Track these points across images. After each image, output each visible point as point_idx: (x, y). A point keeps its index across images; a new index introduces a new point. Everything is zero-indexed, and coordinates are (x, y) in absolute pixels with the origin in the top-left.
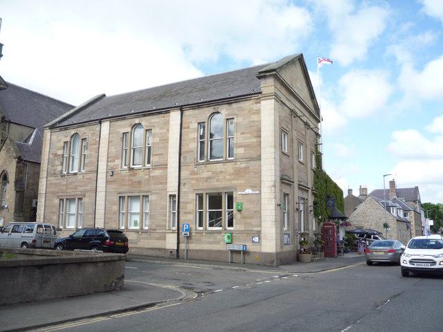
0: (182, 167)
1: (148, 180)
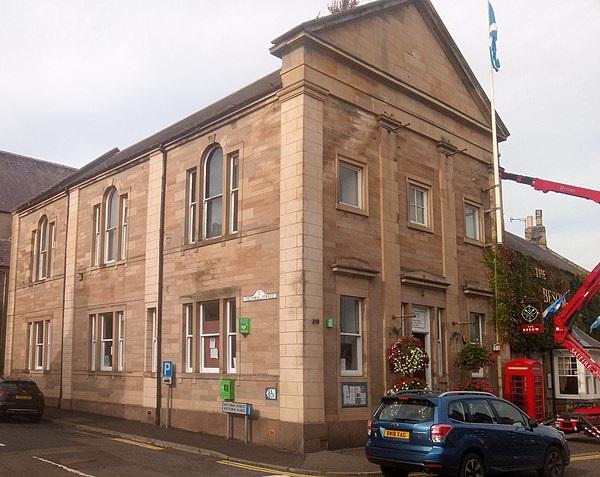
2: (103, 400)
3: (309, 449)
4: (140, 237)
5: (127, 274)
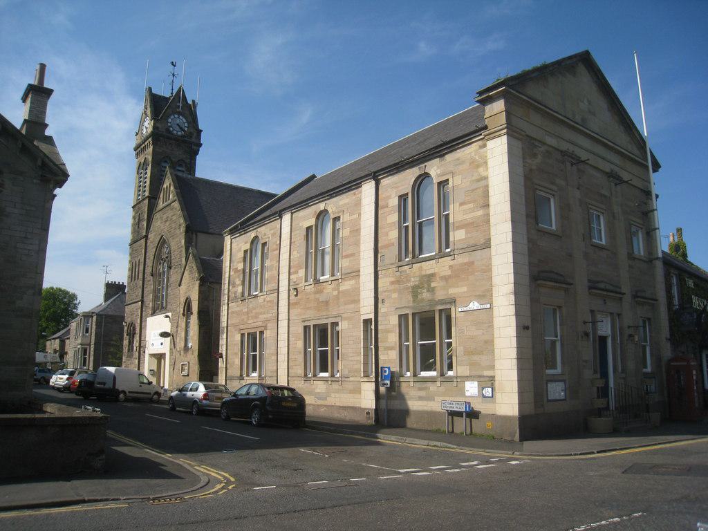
1: (337, 298)
2: (320, 402)
3: (525, 437)
4: (352, 255)
5: (342, 288)
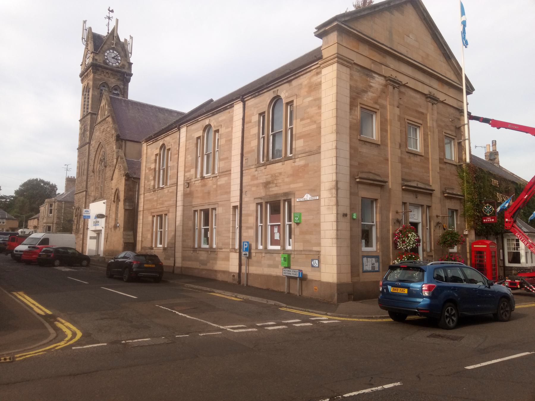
0: (244, 172)
1: (216, 190)
2: (202, 267)
3: (341, 300)
4: (227, 158)
5: (219, 183)
